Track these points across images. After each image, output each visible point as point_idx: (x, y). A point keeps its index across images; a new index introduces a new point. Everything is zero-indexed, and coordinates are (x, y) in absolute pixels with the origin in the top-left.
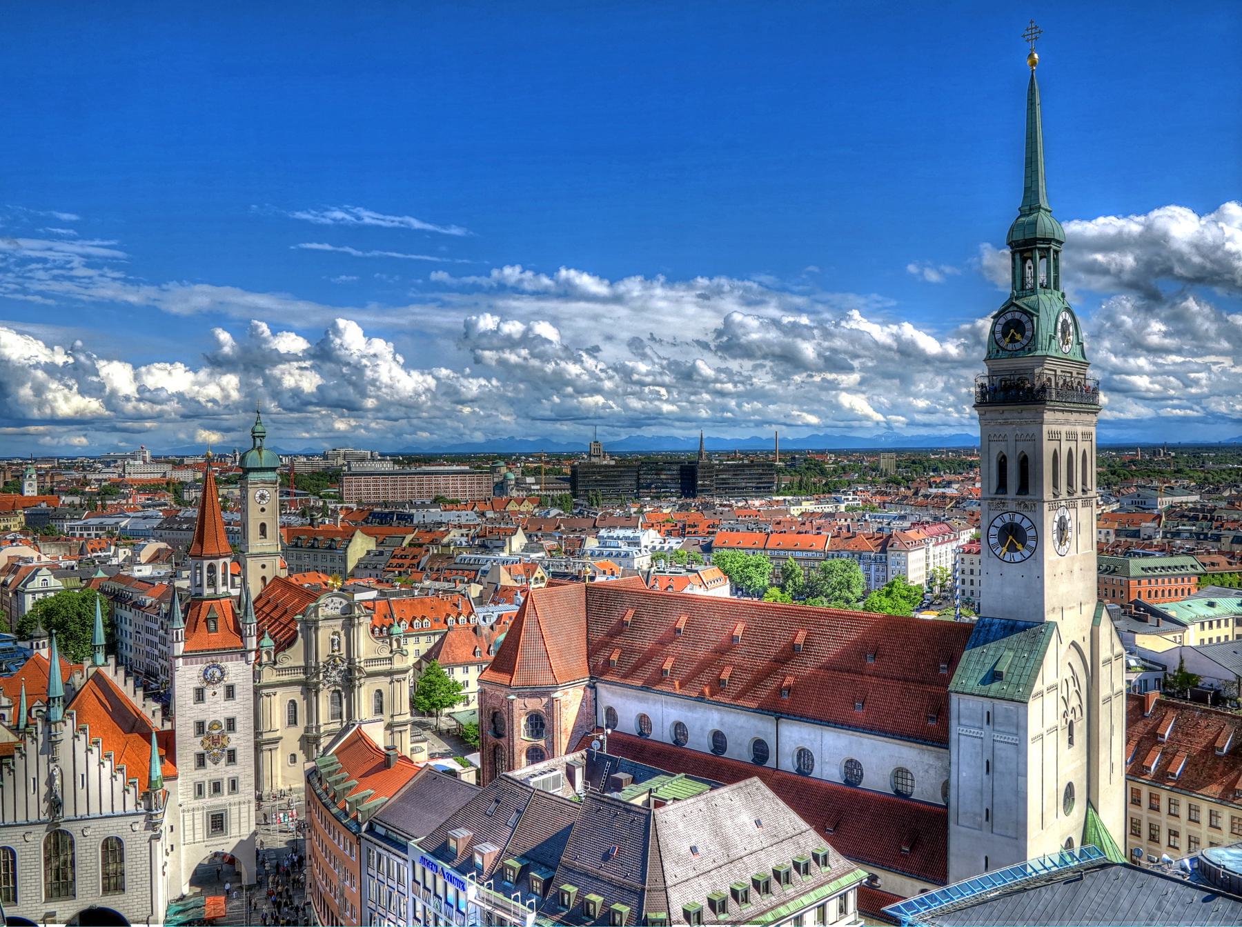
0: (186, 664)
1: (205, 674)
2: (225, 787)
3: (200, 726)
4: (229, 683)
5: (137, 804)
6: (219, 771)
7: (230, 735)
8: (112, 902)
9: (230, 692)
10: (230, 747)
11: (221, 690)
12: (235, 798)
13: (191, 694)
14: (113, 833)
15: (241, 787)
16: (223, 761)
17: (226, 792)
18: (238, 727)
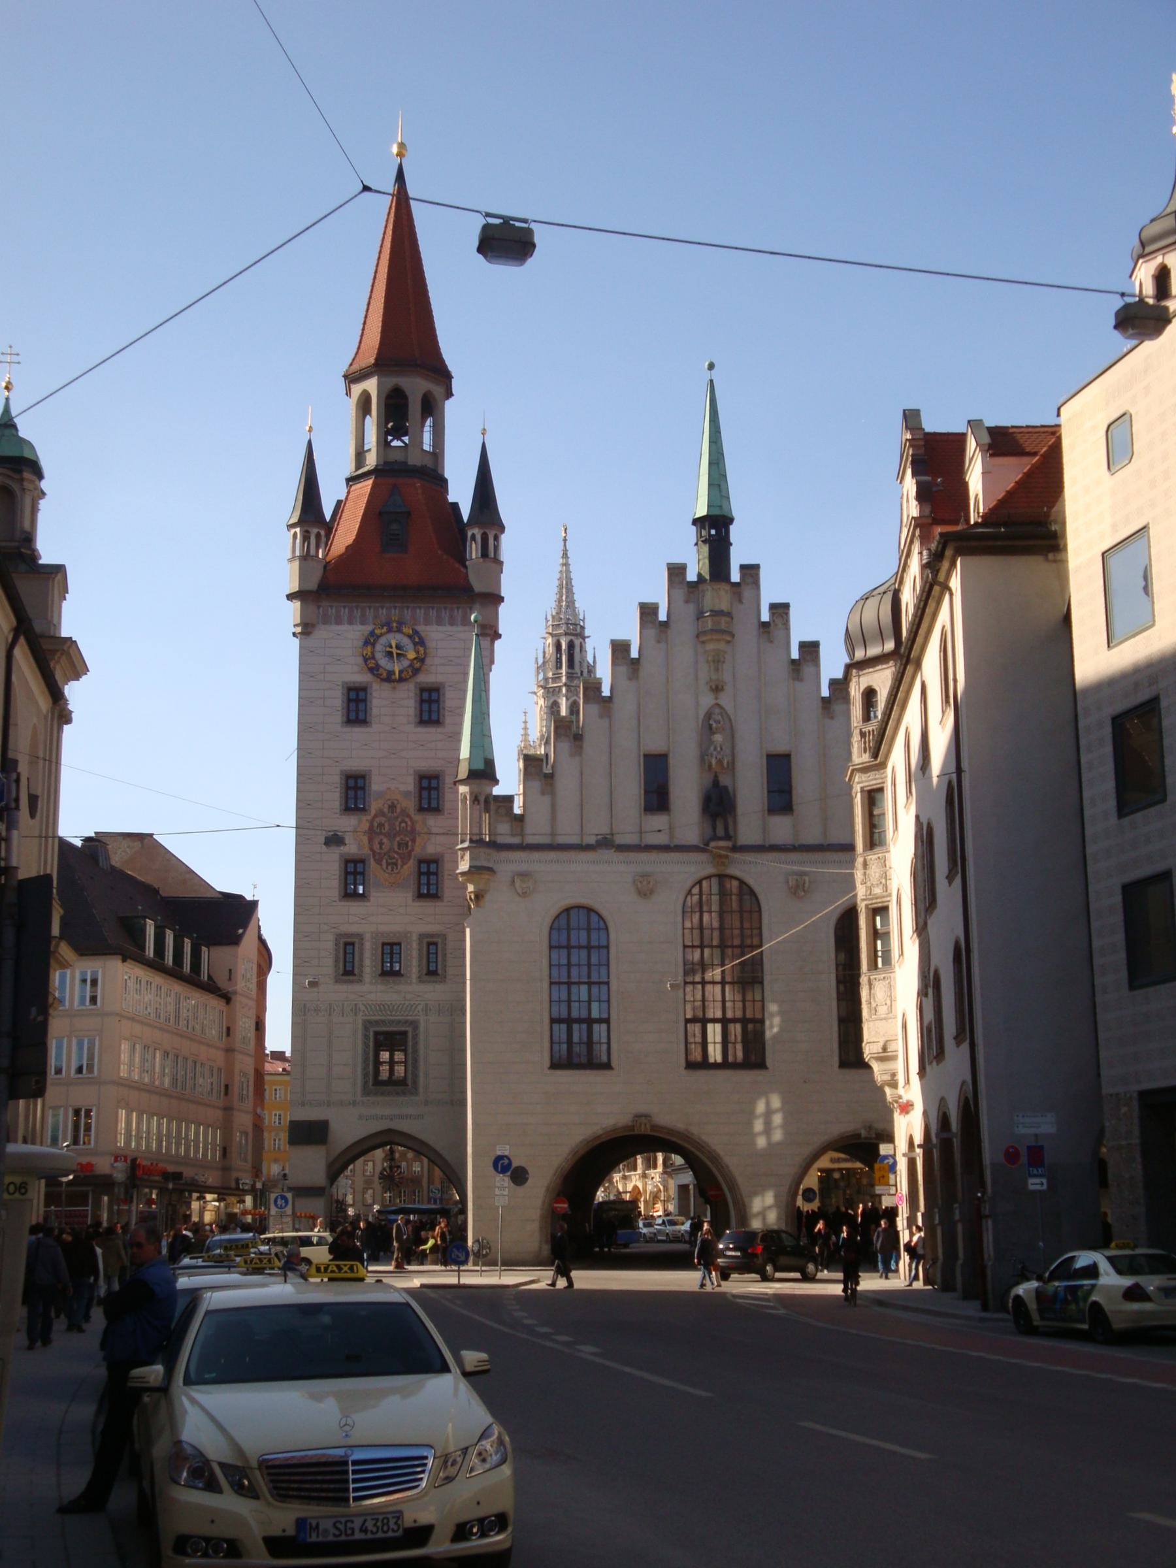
13: (337, 700)
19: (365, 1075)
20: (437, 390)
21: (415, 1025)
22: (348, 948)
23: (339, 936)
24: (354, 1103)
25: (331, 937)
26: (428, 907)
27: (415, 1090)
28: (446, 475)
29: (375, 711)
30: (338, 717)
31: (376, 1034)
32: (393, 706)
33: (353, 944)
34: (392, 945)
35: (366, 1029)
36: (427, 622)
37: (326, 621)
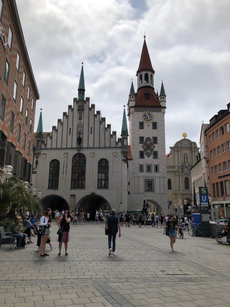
0: (136, 111)
1: (145, 115)
2: (153, 168)
3: (141, 139)
4: (154, 121)
5: (117, 143)
6: (148, 160)
7: (155, 145)
8: (100, 193)
9: (155, 126)
10: (155, 150)
11: (151, 125)
12: (157, 175)
13: (138, 124)
14: (104, 157)
15: (160, 169)
16: (152, 156)
17: (153, 172)
18: (159, 141)
19: (145, 189)
20: (153, 74)
21: (153, 180)
22: (141, 167)
23: (139, 164)
24: (143, 193)
25: (138, 164)
26: (154, 160)
27: (154, 191)
28: (154, 88)
29: (145, 127)
30: (138, 128)
31: (147, 181)
32: (148, 126)
33: (142, 166)
34: (149, 166)
35: (145, 181)
36: (153, 112)
37: (136, 112)
